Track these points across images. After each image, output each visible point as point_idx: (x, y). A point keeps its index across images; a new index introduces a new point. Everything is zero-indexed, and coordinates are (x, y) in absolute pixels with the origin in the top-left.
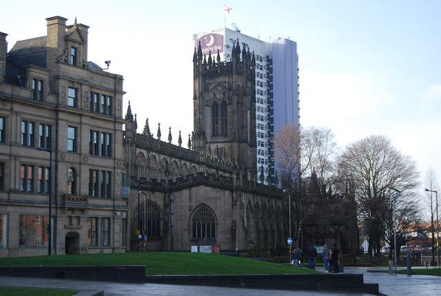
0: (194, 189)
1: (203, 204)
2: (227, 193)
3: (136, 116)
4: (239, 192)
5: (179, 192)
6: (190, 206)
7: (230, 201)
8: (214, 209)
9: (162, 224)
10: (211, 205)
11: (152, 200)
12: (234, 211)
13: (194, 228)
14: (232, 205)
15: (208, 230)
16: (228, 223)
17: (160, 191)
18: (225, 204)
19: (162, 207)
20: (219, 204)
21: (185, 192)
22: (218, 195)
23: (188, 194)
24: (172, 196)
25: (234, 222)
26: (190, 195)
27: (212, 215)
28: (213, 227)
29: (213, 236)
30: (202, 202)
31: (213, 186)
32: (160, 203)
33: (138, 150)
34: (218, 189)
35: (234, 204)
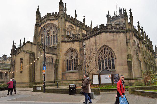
0: (98, 36)
1: (105, 45)
2: (122, 34)
3: (65, 4)
4: (131, 33)
5: (88, 40)
6: (96, 48)
7: (125, 40)
8: (112, 48)
9: (79, 60)
10: (110, 45)
11: (73, 47)
12: (129, 47)
13: (99, 62)
14: (127, 43)
15: (110, 65)
16: (125, 58)
17: (77, 41)
18: (120, 43)
19: (79, 51)
20: (116, 44)
21: (93, 39)
22: (115, 38)
23: (94, 40)
24: (84, 43)
25: (129, 56)
26: (96, 41)
27: (111, 53)
28: (113, 61)
29: (114, 68)
30: (103, 44)
31: (111, 32)
32: (78, 49)
33: (68, 24)
34: (115, 34)
35: (128, 42)
